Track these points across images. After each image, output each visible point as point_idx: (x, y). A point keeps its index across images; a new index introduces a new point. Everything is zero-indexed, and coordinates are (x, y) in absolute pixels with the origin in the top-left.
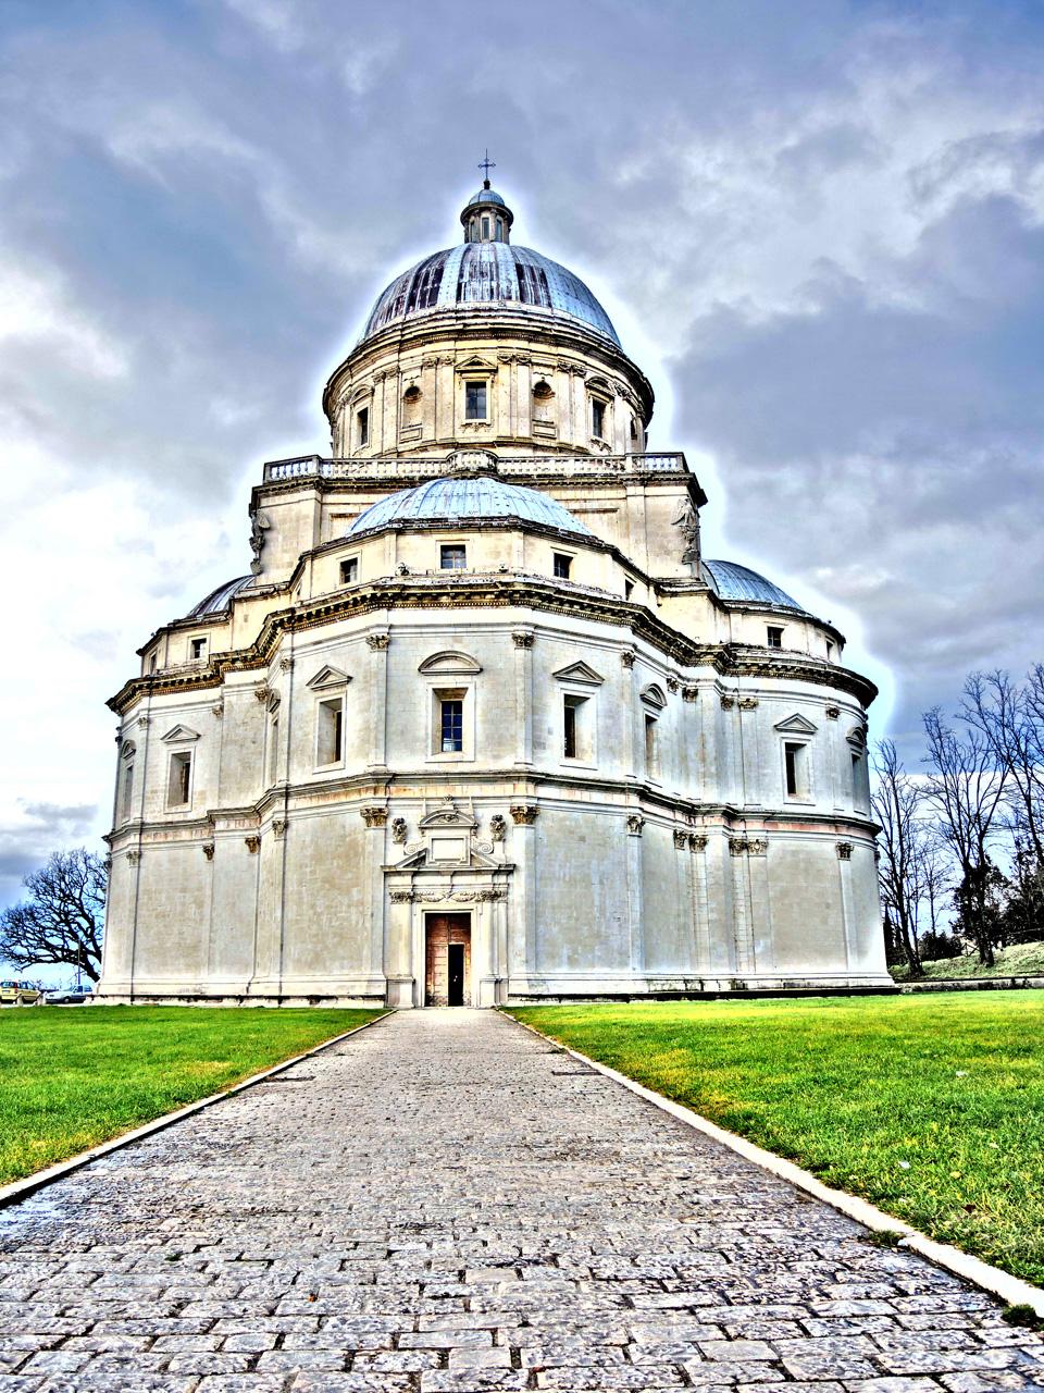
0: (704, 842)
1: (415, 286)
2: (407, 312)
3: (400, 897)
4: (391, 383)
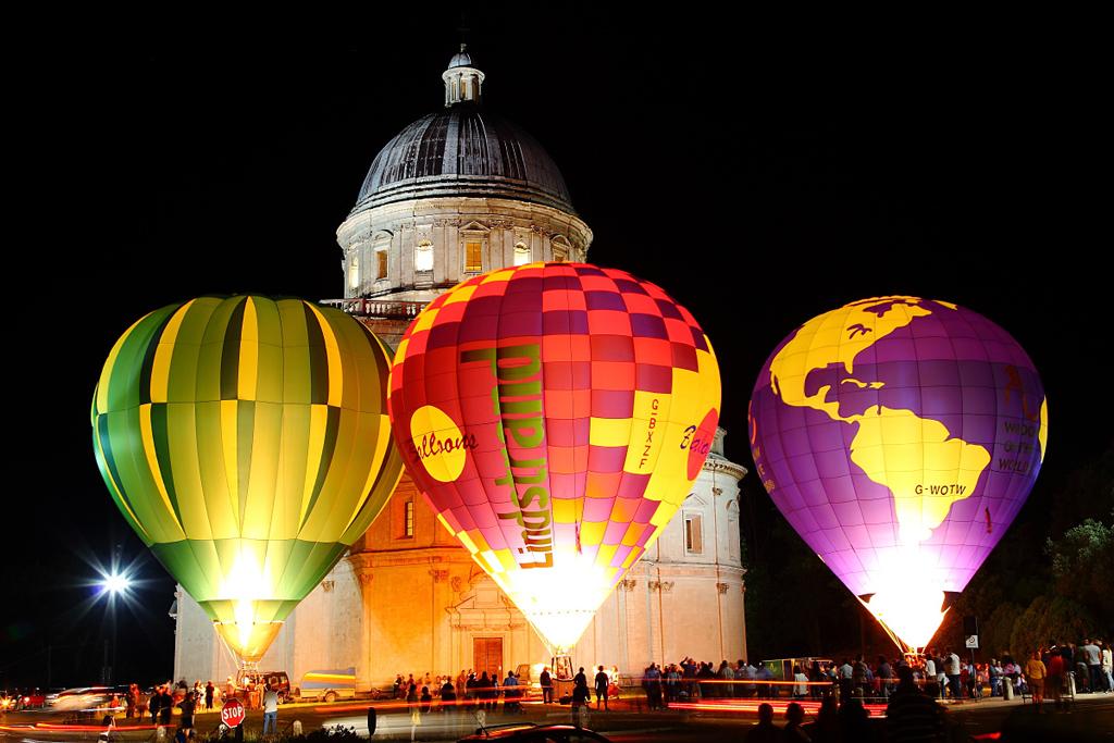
0: (634, 583)
1: (422, 154)
2: (417, 177)
3: (459, 627)
4: (406, 232)
